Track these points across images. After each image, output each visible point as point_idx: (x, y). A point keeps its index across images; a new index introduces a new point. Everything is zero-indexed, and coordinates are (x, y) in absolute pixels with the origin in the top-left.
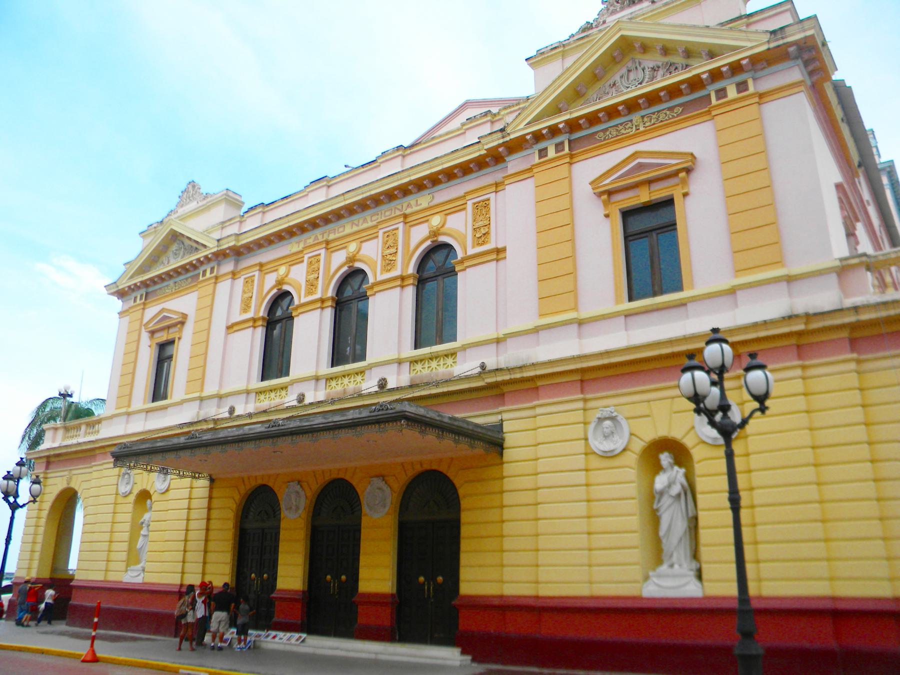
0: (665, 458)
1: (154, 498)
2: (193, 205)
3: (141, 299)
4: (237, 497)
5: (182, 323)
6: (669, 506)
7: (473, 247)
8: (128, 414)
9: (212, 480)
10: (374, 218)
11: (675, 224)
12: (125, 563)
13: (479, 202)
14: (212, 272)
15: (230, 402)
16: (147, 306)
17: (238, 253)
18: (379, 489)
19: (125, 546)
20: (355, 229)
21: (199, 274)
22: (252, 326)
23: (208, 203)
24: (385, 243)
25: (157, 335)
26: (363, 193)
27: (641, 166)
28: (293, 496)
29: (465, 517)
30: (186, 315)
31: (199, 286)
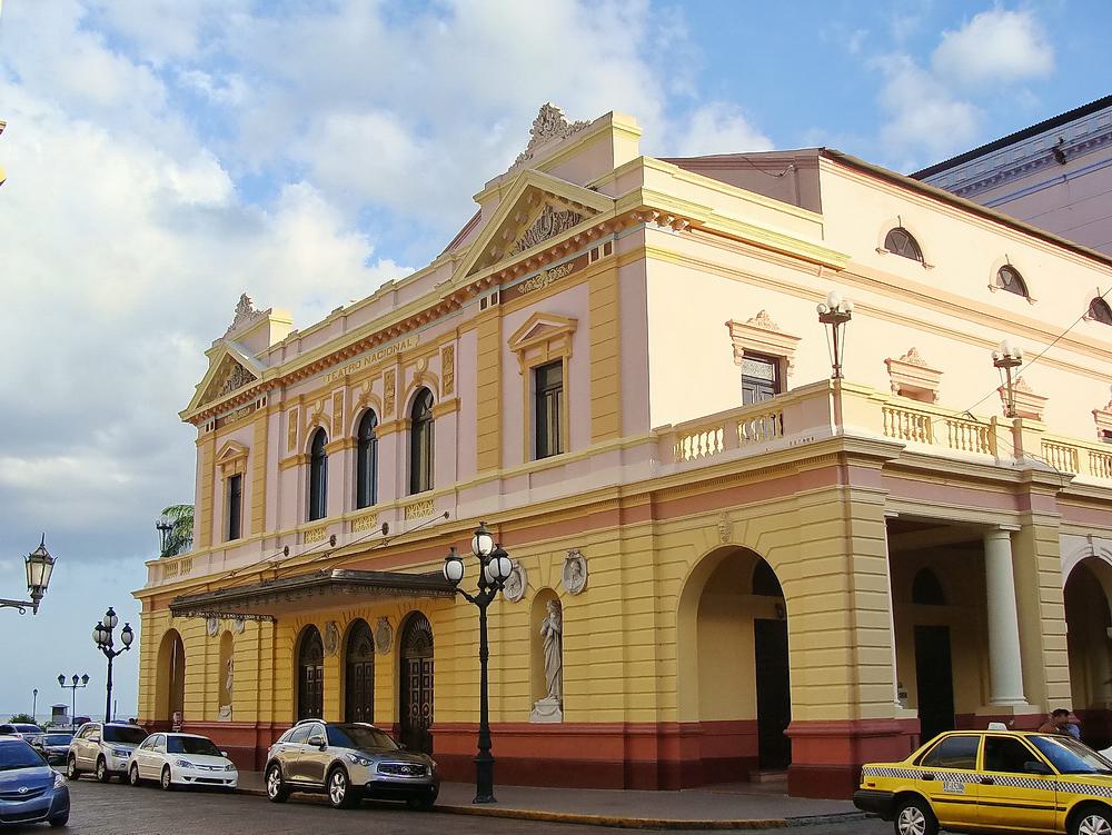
0: (549, 607)
4: (294, 637)
7: (443, 395)
17: (283, 383)
19: (216, 688)
28: (331, 634)
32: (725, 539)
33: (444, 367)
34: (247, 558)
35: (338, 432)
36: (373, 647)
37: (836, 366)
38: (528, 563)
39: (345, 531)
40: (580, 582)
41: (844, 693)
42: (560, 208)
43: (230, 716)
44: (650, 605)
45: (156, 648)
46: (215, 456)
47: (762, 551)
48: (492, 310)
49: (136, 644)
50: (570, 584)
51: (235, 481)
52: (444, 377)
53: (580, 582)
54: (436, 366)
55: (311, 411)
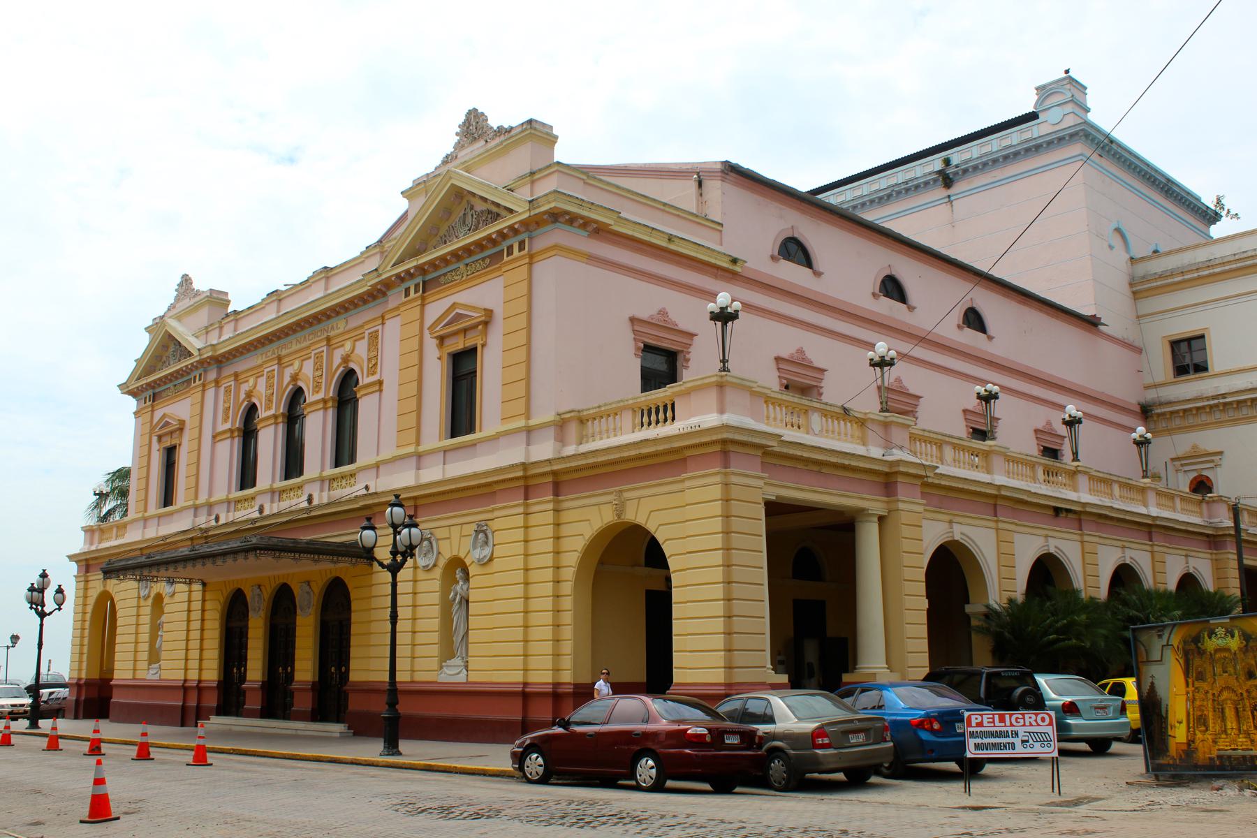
0: (459, 574)
1: (166, 600)
2: (187, 302)
3: (150, 401)
4: (222, 600)
5: (181, 430)
6: (457, 610)
7: (368, 376)
8: (145, 519)
9: (204, 584)
10: (310, 338)
11: (476, 372)
12: (147, 662)
13: (372, 333)
14: (200, 380)
15: (216, 510)
16: (155, 408)
17: (220, 361)
18: (308, 593)
19: (145, 647)
20: (299, 346)
21: (191, 379)
22: (230, 437)
23: (195, 303)
24: (315, 364)
25: (164, 439)
26: (296, 316)
27: (459, 317)
28: (257, 599)
29: (354, 617)
30: (184, 421)
31: (192, 392)
32: (619, 518)
33: (369, 350)
34: (179, 523)
35: (268, 408)
36: (296, 610)
37: (724, 361)
38: (439, 533)
39: (272, 501)
40: (487, 552)
41: (719, 659)
42: (480, 206)
43: (158, 675)
44: (549, 574)
45: (89, 609)
46: (152, 429)
47: (651, 527)
48: (414, 300)
49: (69, 605)
50: (478, 554)
51: (170, 453)
52: (369, 360)
53: (487, 552)
54: (362, 349)
55: (245, 388)
